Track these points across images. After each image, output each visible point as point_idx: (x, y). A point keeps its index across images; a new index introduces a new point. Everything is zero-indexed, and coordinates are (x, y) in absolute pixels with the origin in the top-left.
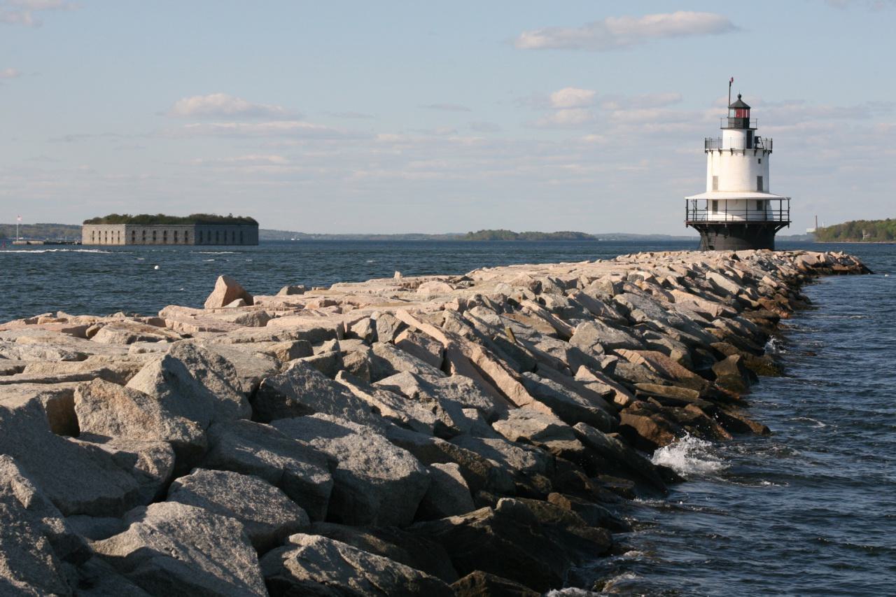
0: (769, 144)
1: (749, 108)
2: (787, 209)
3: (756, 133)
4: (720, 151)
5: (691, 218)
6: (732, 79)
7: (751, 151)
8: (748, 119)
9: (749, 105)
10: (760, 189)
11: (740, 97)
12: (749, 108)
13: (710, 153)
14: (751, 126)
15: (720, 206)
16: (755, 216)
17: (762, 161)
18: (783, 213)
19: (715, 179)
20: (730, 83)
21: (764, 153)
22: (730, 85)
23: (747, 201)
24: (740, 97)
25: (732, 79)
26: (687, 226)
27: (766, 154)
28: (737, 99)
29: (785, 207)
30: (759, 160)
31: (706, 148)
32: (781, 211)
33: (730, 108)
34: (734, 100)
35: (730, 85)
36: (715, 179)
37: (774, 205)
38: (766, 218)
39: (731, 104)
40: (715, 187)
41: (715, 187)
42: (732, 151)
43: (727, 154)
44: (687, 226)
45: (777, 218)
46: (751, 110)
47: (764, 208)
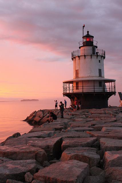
1: (93, 37)
6: (84, 25)
11: (88, 32)
15: (80, 85)
16: (98, 90)
17: (101, 61)
18: (112, 87)
22: (83, 28)
24: (88, 32)
25: (84, 25)
27: (103, 58)
30: (99, 61)
31: (72, 57)
32: (112, 86)
34: (85, 34)
35: (83, 28)
43: (82, 58)
45: (108, 90)
47: (102, 85)
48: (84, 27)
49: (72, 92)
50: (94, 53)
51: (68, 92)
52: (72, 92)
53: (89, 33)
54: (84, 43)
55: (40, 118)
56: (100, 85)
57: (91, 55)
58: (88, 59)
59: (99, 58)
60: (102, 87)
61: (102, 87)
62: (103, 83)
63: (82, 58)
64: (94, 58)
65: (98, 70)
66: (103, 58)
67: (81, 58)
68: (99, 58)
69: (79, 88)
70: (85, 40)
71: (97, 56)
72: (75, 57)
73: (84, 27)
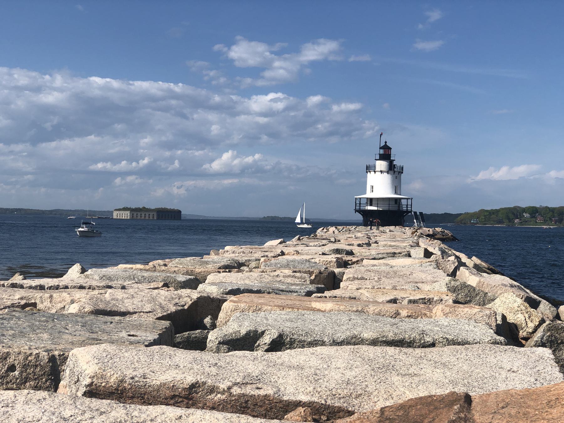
1: (391, 149)
3: (395, 163)
4: (375, 172)
7: (392, 172)
8: (390, 154)
11: (386, 142)
12: (391, 149)
14: (392, 159)
15: (374, 202)
16: (394, 207)
20: (381, 135)
23: (389, 199)
24: (386, 142)
29: (409, 203)
30: (396, 177)
33: (380, 148)
34: (383, 144)
37: (404, 202)
42: (381, 172)
45: (405, 209)
58: (386, 174)
62: (398, 201)
70: (382, 152)
71: (394, 172)
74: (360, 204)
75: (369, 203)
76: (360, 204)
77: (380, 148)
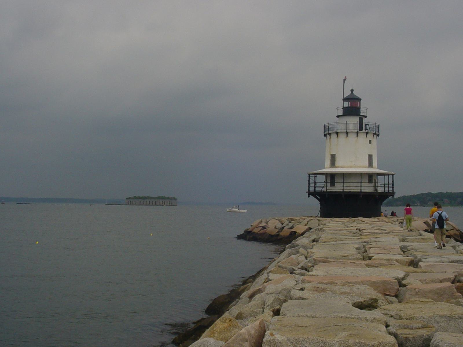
0: (377, 129)
1: (360, 100)
2: (388, 182)
3: (365, 121)
5: (312, 189)
6: (346, 77)
9: (361, 98)
10: (370, 165)
11: (352, 91)
12: (360, 100)
13: (328, 136)
15: (337, 180)
16: (368, 188)
17: (372, 142)
19: (333, 157)
21: (373, 136)
24: (352, 91)
25: (346, 77)
26: (309, 196)
27: (375, 136)
28: (350, 92)
30: (370, 141)
34: (347, 93)
36: (333, 157)
38: (376, 190)
39: (345, 96)
40: (333, 164)
41: (333, 164)
44: (309, 196)
46: (361, 101)
47: (373, 181)
48: (345, 80)
49: (326, 191)
50: (361, 128)
51: (318, 189)
52: (324, 190)
53: (354, 92)
54: (344, 108)
55: (278, 230)
56: (370, 181)
57: (357, 133)
58: (352, 137)
59: (370, 136)
60: (373, 185)
61: (373, 185)
62: (374, 178)
63: (342, 137)
64: (362, 136)
65: (368, 156)
66: (375, 136)
67: (340, 135)
68: (370, 136)
69: (336, 184)
70: (347, 104)
71: (367, 133)
72: (330, 133)
73: (345, 80)
74: (315, 183)
75: (329, 181)
76: (315, 183)
77: (345, 100)
